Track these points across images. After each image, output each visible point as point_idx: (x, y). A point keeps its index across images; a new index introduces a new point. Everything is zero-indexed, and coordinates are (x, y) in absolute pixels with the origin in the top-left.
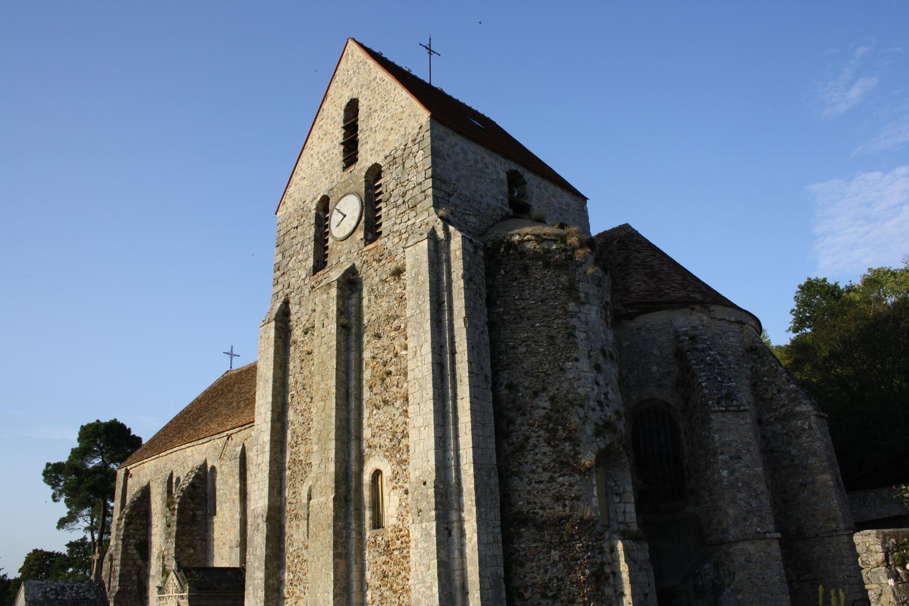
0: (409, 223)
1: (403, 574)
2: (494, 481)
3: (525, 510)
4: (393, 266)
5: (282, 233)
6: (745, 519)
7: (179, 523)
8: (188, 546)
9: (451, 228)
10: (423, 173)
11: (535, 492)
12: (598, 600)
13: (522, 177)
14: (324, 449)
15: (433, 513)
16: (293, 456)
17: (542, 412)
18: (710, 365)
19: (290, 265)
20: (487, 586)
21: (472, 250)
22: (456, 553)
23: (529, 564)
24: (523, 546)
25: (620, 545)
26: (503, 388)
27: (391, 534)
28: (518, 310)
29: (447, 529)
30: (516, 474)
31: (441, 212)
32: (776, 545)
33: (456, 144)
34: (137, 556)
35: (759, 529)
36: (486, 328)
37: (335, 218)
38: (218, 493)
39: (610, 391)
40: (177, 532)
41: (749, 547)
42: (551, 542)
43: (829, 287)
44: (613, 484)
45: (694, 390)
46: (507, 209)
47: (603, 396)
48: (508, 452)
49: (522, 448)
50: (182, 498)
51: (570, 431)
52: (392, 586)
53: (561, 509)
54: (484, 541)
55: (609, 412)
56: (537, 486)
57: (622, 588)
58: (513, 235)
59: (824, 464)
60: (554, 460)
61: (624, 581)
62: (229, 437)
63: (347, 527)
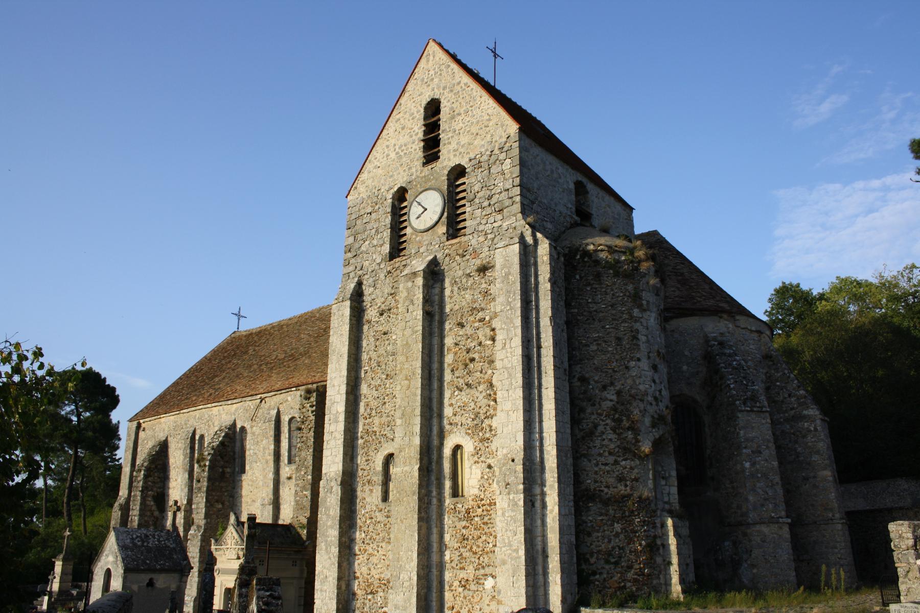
0: (495, 225)
1: (484, 538)
2: (570, 461)
3: (592, 488)
4: (478, 262)
5: (353, 217)
6: (763, 505)
7: (210, 479)
8: (217, 501)
9: (539, 235)
10: (511, 181)
13: (585, 187)
14: (408, 424)
15: (521, 487)
16: (366, 427)
17: (610, 404)
18: (736, 369)
19: (363, 248)
20: (564, 551)
21: (556, 256)
22: (539, 522)
23: (595, 534)
24: (590, 518)
25: (670, 522)
26: (576, 380)
27: (471, 503)
28: (591, 312)
30: (585, 456)
31: (529, 219)
32: (786, 529)
34: (154, 508)
37: (415, 210)
38: (247, 453)
40: (208, 487)
41: (765, 529)
43: (802, 292)
44: (660, 469)
45: (721, 390)
46: (577, 218)
47: (658, 393)
48: (579, 437)
49: (591, 434)
50: (213, 455)
51: (633, 422)
52: (471, 548)
53: (623, 488)
54: (563, 513)
55: (662, 406)
56: (603, 467)
57: (670, 558)
58: (587, 244)
59: (826, 462)
60: (618, 446)
62: (262, 400)
63: (429, 493)
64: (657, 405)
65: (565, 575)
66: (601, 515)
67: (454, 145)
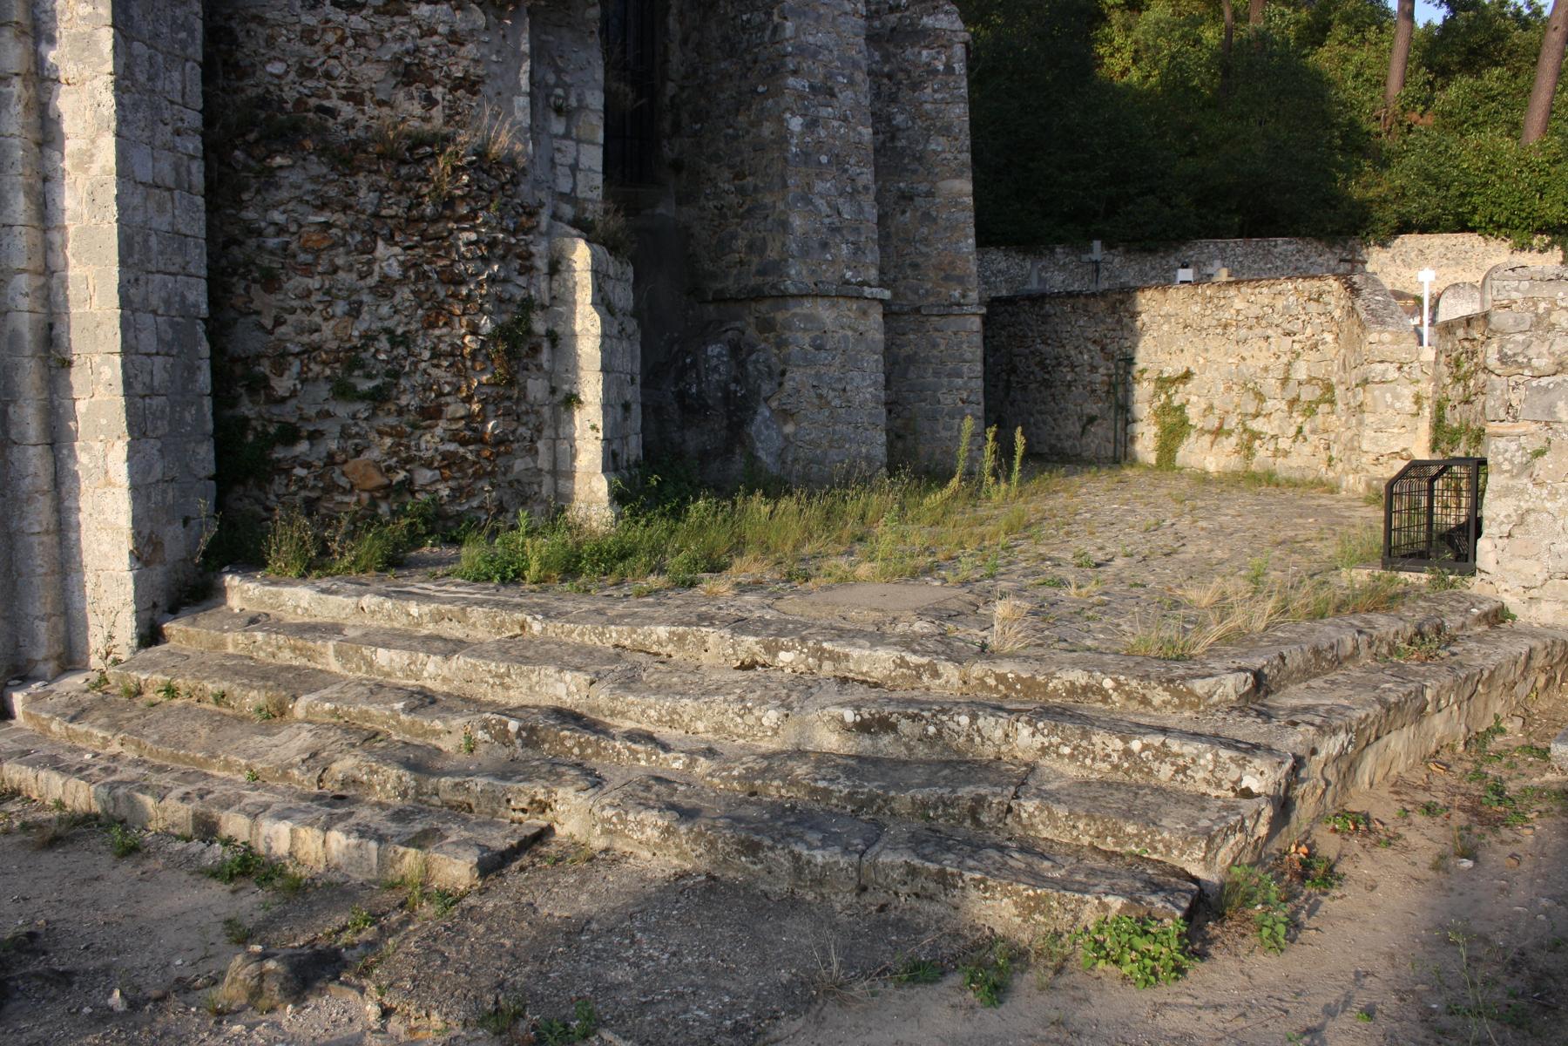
3: (290, 95)
6: (825, 246)
11: (331, 38)
12: (507, 413)
20: (148, 342)
23: (296, 282)
24: (277, 216)
25: (581, 255)
32: (876, 315)
35: (849, 274)
41: (825, 313)
42: (376, 215)
44: (551, 78)
53: (417, 110)
54: (144, 173)
61: (582, 362)
65: (152, 446)
66: (323, 206)
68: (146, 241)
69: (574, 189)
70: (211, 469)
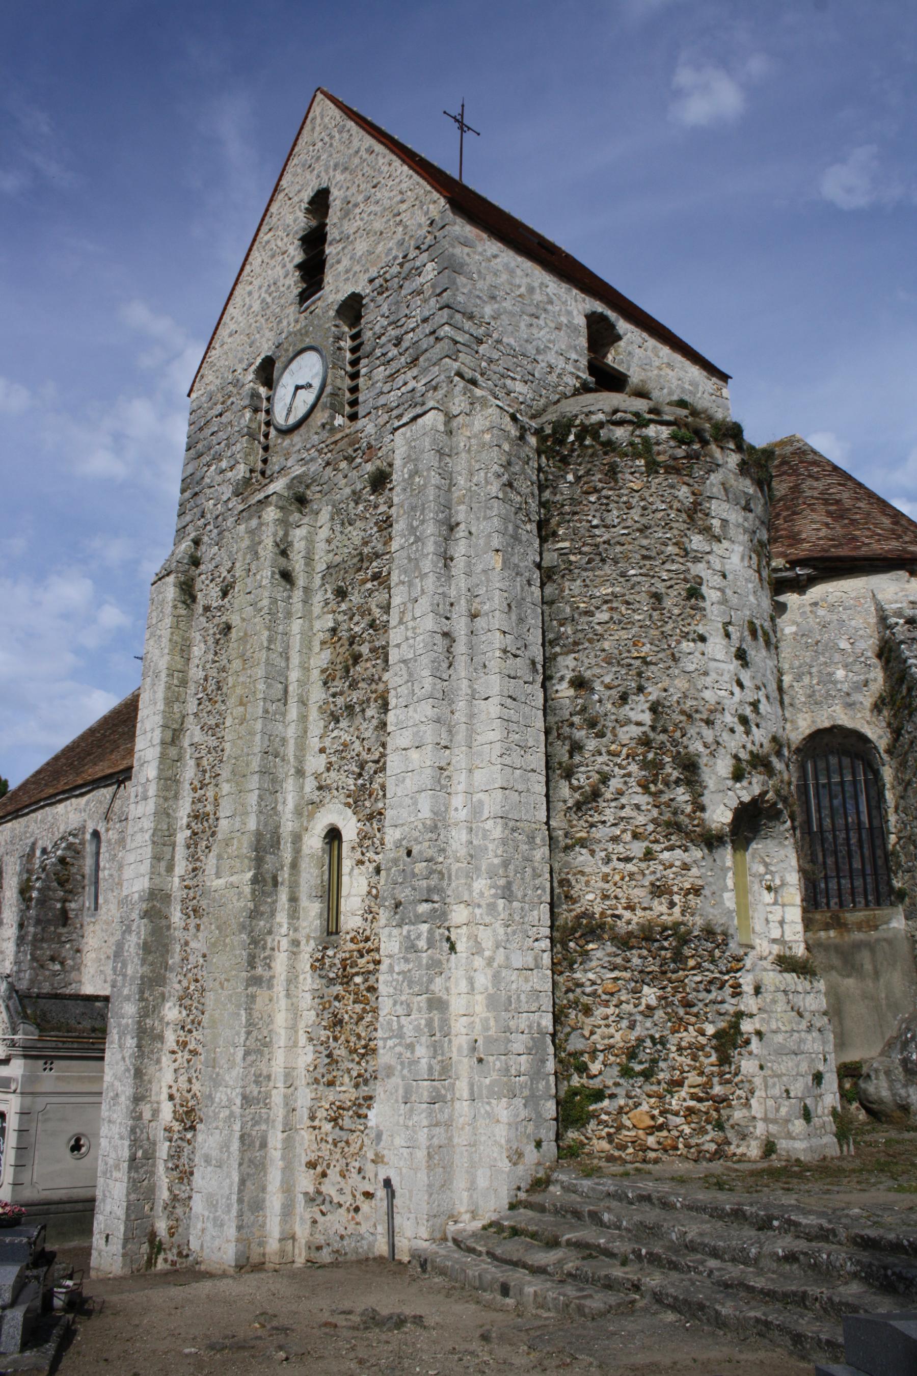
3: (597, 910)
8: (53, 959)
11: (617, 878)
13: (612, 326)
17: (635, 731)
19: (207, 480)
21: (514, 432)
23: (600, 1011)
24: (591, 976)
28: (597, 546)
29: (448, 939)
33: (495, 256)
36: (536, 575)
39: (763, 700)
44: (762, 869)
46: (585, 375)
53: (664, 909)
56: (621, 865)
60: (654, 821)
64: (748, 733)
67: (346, 262)
68: (519, 997)
69: (783, 936)
70: (553, 1114)
